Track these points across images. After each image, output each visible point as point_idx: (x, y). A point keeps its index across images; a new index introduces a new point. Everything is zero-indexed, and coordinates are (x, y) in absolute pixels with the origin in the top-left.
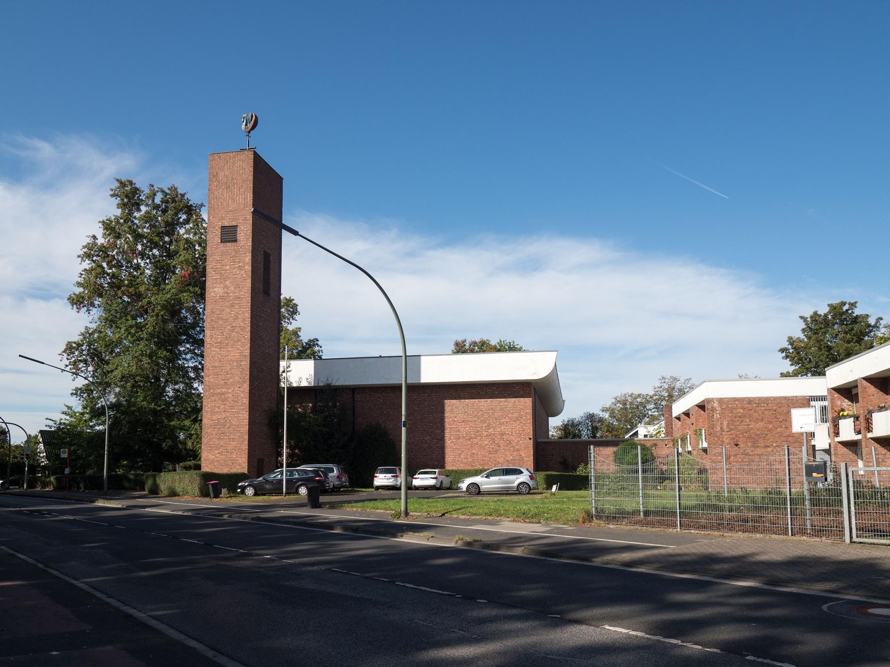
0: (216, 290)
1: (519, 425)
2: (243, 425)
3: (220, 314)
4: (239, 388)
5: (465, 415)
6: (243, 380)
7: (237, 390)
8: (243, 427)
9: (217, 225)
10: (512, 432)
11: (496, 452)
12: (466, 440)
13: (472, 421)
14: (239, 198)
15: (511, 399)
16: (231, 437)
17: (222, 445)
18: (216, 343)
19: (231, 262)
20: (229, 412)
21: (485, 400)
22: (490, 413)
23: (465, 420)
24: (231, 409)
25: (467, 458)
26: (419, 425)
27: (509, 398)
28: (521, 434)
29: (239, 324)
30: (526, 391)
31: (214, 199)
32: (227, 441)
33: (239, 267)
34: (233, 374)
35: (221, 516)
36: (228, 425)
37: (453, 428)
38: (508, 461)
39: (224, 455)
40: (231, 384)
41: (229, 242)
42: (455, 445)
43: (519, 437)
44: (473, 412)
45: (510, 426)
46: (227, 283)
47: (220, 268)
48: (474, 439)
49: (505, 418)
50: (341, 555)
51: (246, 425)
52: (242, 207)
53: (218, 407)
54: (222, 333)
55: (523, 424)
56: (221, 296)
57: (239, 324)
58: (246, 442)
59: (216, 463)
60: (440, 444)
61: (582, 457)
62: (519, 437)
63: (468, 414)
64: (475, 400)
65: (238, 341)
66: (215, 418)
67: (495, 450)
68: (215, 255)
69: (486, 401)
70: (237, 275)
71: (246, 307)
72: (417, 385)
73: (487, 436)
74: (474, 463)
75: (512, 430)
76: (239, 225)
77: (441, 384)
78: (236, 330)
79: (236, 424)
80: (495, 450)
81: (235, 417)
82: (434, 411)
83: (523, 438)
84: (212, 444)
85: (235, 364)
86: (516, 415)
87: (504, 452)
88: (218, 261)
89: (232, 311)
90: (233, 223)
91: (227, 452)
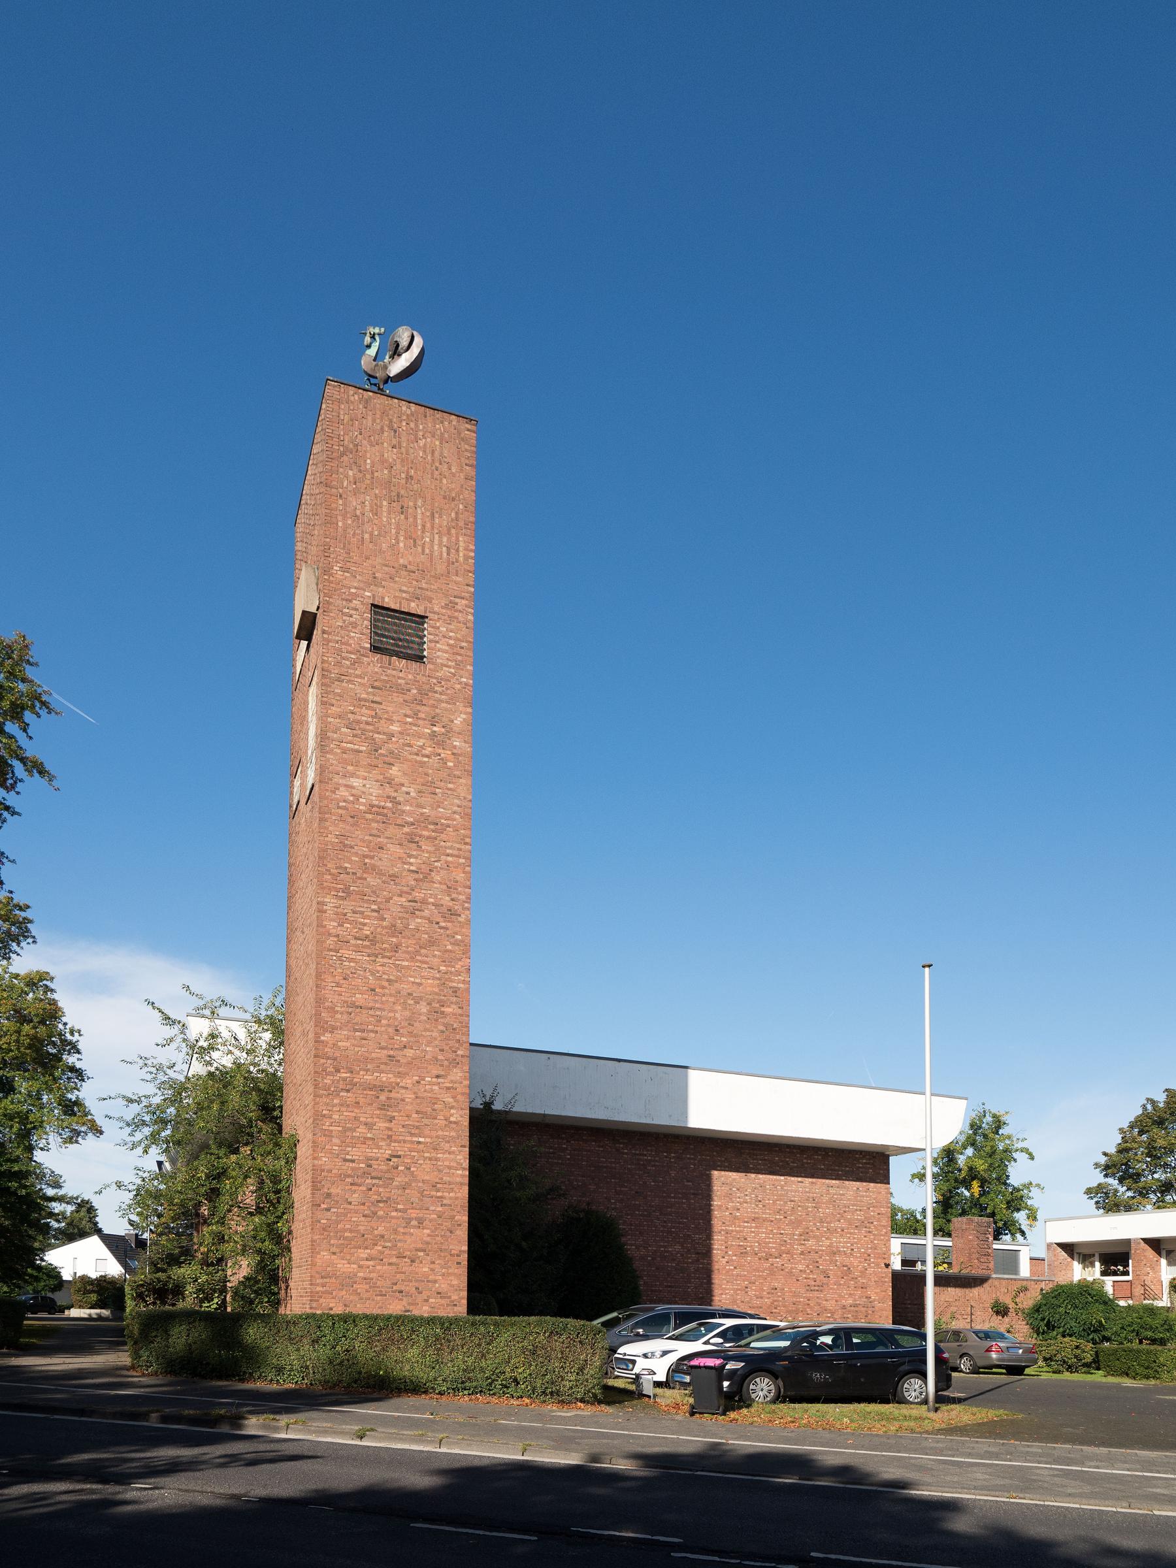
0: (356, 782)
1: (865, 1237)
2: (450, 1183)
3: (372, 858)
4: (438, 1077)
5: (757, 1206)
6: (452, 1056)
7: (430, 1084)
8: (452, 1190)
9: (355, 596)
10: (852, 1250)
11: (821, 1287)
12: (760, 1259)
13: (772, 1221)
14: (432, 541)
15: (851, 1183)
16: (413, 1213)
17: (382, 1236)
18: (356, 938)
19: (406, 716)
20: (405, 1142)
21: (800, 1179)
22: (808, 1207)
23: (757, 1218)
24: (412, 1135)
25: (762, 1298)
26: (658, 1219)
27: (846, 1180)
28: (869, 1255)
29: (436, 898)
30: (880, 1169)
31: (345, 518)
32: (399, 1226)
33: (433, 735)
34: (415, 1036)
35: (144, 1416)
36: (399, 1180)
37: (732, 1231)
38: (844, 1307)
39: (390, 1264)
40: (409, 1063)
41: (400, 655)
42: (735, 1268)
43: (866, 1260)
44: (774, 1201)
45: (849, 1238)
46: (394, 771)
47: (367, 723)
48: (776, 1258)
49: (839, 1221)
50: (113, 1452)
51: (461, 1184)
52: (441, 568)
53: (369, 1126)
54: (378, 911)
55: (874, 1235)
56: (372, 806)
57: (436, 898)
58: (463, 1233)
59: (361, 1288)
60: (703, 1264)
61: (905, 1304)
62: (866, 1260)
63: (764, 1206)
64: (778, 1177)
65: (432, 943)
66: (354, 1153)
67: (820, 1284)
68: (349, 681)
69: (802, 1182)
70: (427, 756)
71: (456, 852)
72: (677, 1132)
73: (802, 1253)
74: (776, 1308)
75: (852, 1245)
76: (431, 615)
77: (708, 1135)
78: (426, 913)
79: (427, 1178)
80: (818, 1283)
81: (425, 1158)
82: (692, 1191)
83: (873, 1263)
84: (346, 1230)
85: (423, 1008)
86: (859, 1216)
87: (838, 1289)
88: (360, 700)
89: (410, 856)
90: (413, 604)
91: (401, 1256)
